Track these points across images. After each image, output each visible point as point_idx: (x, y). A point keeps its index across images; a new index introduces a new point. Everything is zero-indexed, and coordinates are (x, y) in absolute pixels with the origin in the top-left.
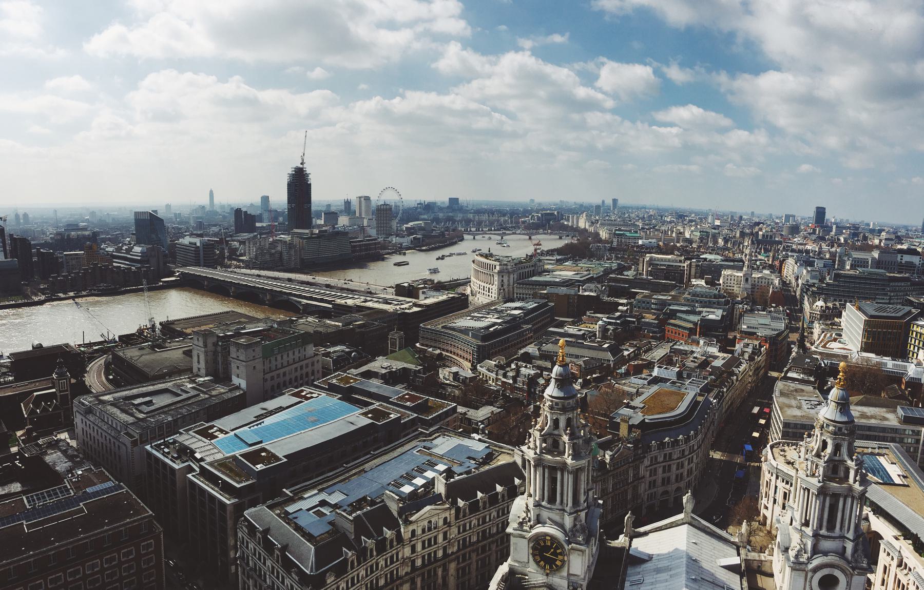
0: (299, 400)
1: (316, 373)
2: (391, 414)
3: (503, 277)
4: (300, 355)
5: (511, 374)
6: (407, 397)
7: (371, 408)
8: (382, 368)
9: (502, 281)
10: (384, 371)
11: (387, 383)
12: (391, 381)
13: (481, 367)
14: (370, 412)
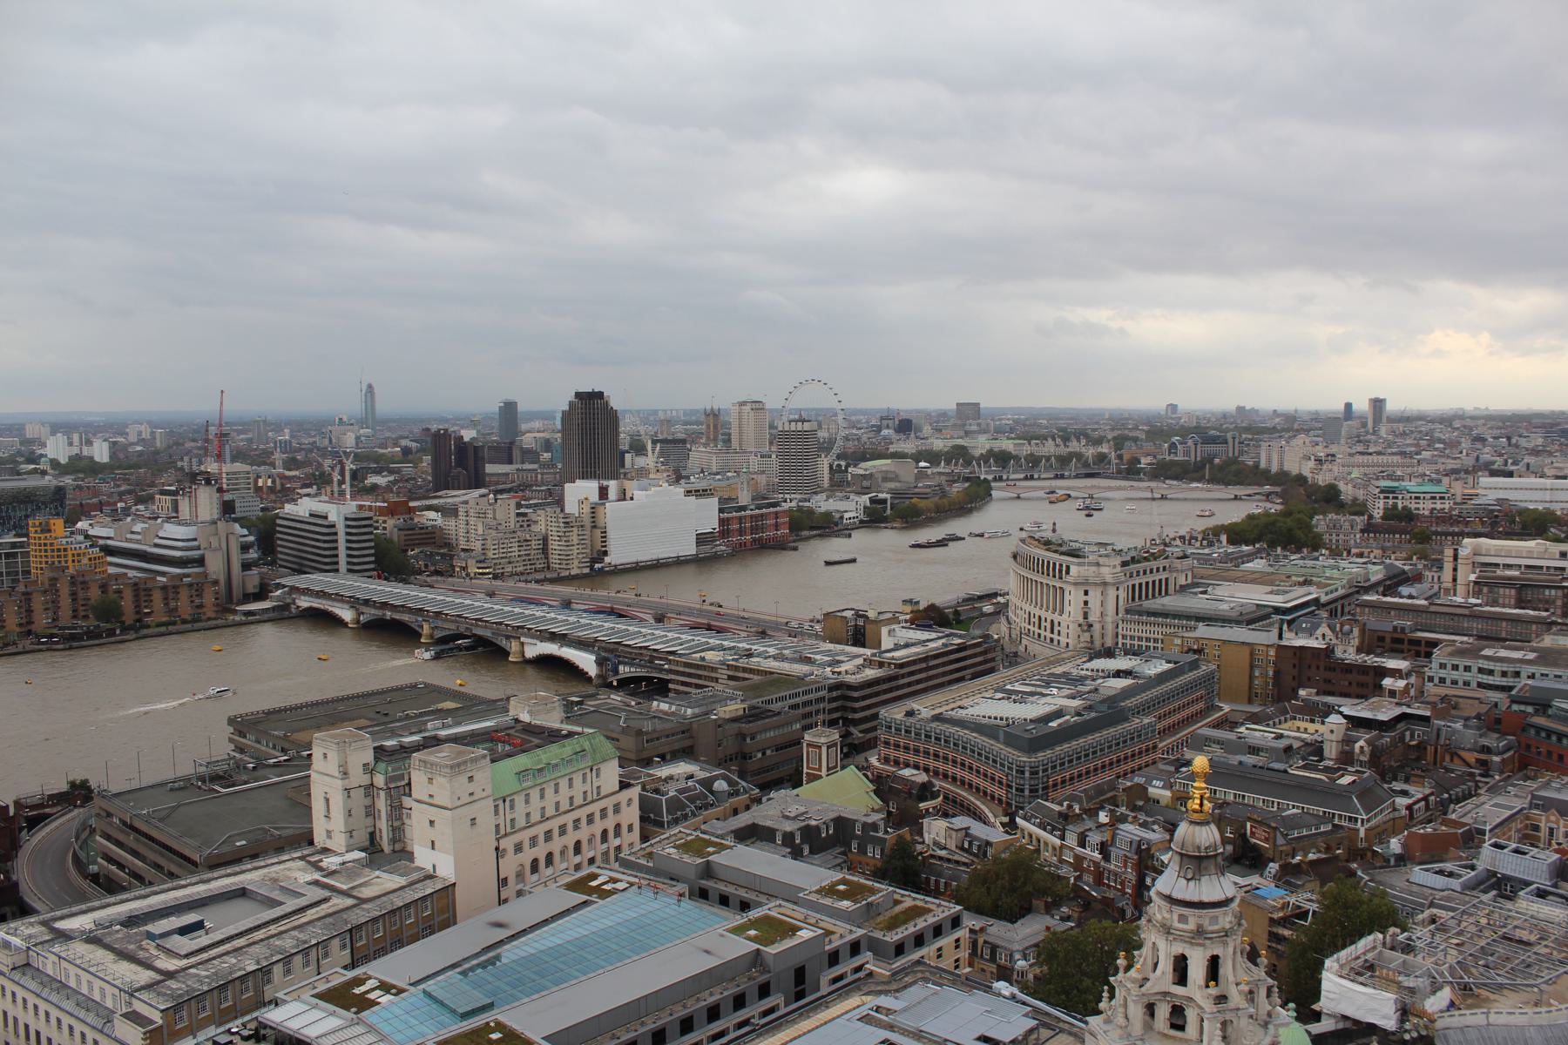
0: (585, 898)
1: (624, 829)
2: (800, 929)
3: (1086, 593)
4: (587, 787)
5: (1095, 838)
6: (842, 887)
7: (754, 914)
8: (787, 818)
9: (1086, 603)
10: (789, 827)
11: (796, 854)
12: (806, 851)
13: (1025, 818)
14: (753, 924)
